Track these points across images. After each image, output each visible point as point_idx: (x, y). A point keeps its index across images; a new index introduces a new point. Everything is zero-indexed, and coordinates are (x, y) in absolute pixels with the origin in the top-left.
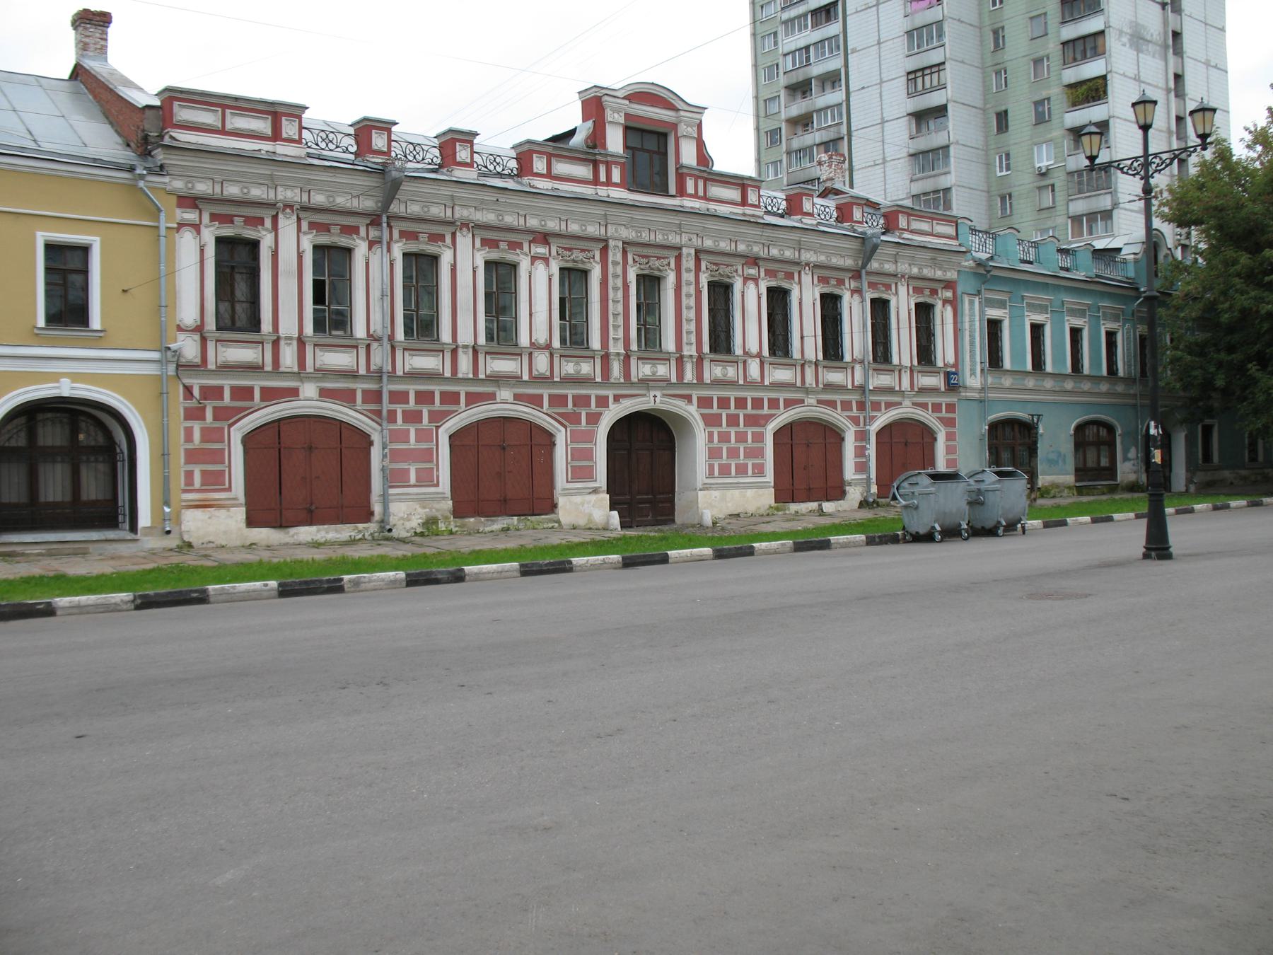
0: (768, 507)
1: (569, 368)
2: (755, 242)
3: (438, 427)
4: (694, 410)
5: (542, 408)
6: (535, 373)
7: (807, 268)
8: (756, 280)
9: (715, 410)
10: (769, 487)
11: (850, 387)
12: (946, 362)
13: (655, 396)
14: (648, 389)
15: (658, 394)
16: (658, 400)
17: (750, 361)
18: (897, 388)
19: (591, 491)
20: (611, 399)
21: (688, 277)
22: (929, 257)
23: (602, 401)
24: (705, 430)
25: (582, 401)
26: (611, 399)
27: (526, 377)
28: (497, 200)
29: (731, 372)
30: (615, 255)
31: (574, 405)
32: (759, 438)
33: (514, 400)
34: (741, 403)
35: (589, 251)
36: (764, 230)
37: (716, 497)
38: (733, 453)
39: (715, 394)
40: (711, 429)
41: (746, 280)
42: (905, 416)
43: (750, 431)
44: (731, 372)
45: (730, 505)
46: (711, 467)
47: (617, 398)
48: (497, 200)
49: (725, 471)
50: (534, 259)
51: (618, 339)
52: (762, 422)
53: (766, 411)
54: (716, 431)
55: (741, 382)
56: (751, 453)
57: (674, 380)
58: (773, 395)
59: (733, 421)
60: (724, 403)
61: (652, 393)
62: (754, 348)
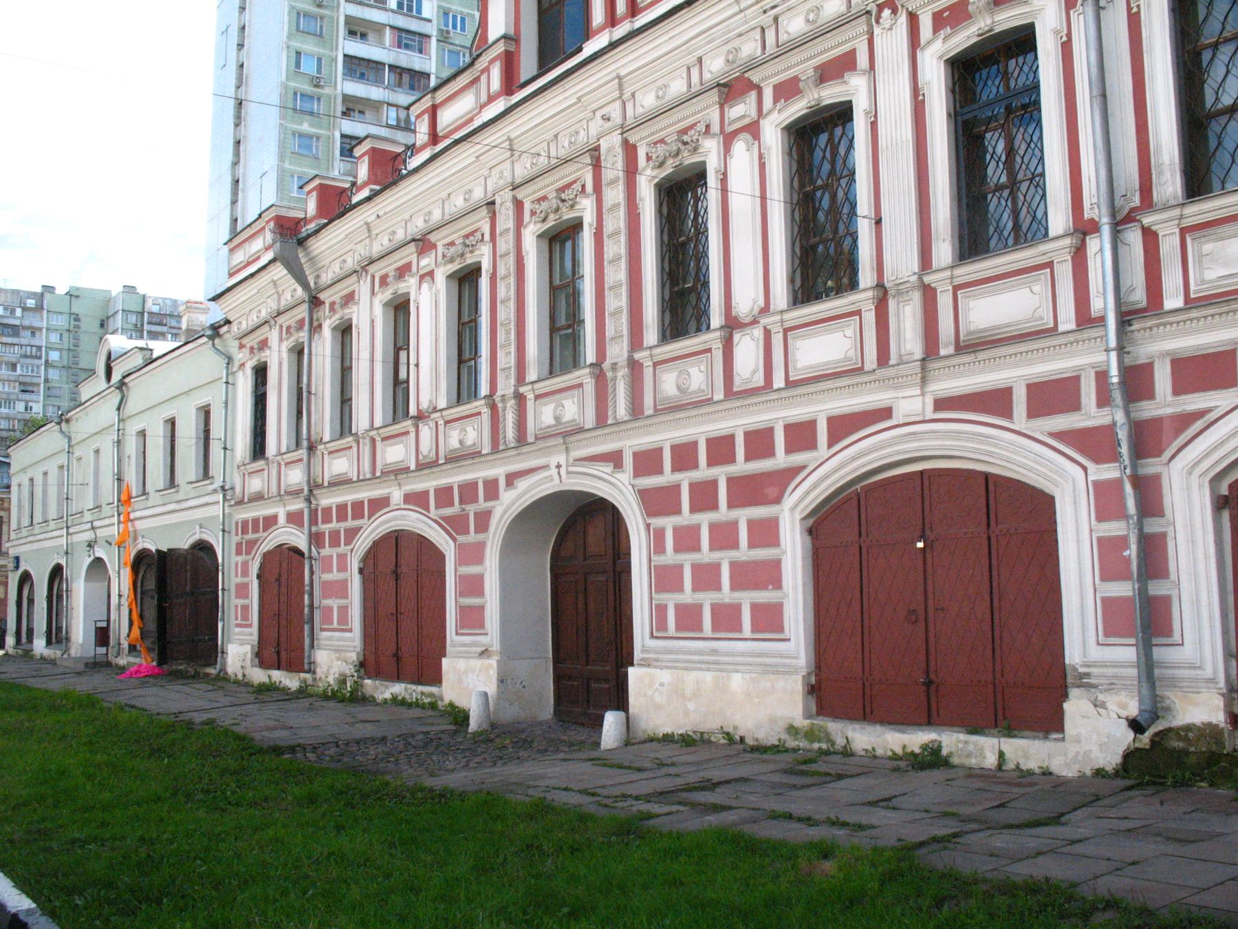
0: (782, 725)
1: (452, 439)
2: (740, 35)
3: (352, 550)
4: (627, 483)
5: (429, 512)
6: (421, 457)
7: (887, 13)
8: (753, 129)
9: (668, 477)
10: (796, 672)
11: (1067, 321)
13: (559, 466)
14: (547, 451)
15: (561, 459)
16: (563, 471)
17: (737, 337)
19: (480, 649)
20: (502, 482)
21: (615, 195)
23: (492, 488)
24: (648, 526)
25: (468, 492)
26: (502, 482)
27: (413, 467)
28: (378, 216)
29: (697, 377)
30: (506, 220)
31: (462, 502)
32: (766, 533)
33: (405, 502)
34: (721, 449)
35: (476, 231)
37: (662, 685)
38: (706, 577)
39: (665, 436)
40: (657, 522)
41: (728, 139)
43: (744, 516)
44: (697, 377)
45: (691, 706)
46: (661, 610)
47: (511, 479)
48: (378, 216)
49: (689, 619)
50: (422, 277)
51: (510, 368)
52: (771, 491)
53: (781, 459)
54: (668, 523)
55: (719, 395)
56: (746, 576)
57: (590, 420)
58: (798, 413)
59: (704, 497)
60: (684, 456)
61: (553, 461)
62: (746, 299)
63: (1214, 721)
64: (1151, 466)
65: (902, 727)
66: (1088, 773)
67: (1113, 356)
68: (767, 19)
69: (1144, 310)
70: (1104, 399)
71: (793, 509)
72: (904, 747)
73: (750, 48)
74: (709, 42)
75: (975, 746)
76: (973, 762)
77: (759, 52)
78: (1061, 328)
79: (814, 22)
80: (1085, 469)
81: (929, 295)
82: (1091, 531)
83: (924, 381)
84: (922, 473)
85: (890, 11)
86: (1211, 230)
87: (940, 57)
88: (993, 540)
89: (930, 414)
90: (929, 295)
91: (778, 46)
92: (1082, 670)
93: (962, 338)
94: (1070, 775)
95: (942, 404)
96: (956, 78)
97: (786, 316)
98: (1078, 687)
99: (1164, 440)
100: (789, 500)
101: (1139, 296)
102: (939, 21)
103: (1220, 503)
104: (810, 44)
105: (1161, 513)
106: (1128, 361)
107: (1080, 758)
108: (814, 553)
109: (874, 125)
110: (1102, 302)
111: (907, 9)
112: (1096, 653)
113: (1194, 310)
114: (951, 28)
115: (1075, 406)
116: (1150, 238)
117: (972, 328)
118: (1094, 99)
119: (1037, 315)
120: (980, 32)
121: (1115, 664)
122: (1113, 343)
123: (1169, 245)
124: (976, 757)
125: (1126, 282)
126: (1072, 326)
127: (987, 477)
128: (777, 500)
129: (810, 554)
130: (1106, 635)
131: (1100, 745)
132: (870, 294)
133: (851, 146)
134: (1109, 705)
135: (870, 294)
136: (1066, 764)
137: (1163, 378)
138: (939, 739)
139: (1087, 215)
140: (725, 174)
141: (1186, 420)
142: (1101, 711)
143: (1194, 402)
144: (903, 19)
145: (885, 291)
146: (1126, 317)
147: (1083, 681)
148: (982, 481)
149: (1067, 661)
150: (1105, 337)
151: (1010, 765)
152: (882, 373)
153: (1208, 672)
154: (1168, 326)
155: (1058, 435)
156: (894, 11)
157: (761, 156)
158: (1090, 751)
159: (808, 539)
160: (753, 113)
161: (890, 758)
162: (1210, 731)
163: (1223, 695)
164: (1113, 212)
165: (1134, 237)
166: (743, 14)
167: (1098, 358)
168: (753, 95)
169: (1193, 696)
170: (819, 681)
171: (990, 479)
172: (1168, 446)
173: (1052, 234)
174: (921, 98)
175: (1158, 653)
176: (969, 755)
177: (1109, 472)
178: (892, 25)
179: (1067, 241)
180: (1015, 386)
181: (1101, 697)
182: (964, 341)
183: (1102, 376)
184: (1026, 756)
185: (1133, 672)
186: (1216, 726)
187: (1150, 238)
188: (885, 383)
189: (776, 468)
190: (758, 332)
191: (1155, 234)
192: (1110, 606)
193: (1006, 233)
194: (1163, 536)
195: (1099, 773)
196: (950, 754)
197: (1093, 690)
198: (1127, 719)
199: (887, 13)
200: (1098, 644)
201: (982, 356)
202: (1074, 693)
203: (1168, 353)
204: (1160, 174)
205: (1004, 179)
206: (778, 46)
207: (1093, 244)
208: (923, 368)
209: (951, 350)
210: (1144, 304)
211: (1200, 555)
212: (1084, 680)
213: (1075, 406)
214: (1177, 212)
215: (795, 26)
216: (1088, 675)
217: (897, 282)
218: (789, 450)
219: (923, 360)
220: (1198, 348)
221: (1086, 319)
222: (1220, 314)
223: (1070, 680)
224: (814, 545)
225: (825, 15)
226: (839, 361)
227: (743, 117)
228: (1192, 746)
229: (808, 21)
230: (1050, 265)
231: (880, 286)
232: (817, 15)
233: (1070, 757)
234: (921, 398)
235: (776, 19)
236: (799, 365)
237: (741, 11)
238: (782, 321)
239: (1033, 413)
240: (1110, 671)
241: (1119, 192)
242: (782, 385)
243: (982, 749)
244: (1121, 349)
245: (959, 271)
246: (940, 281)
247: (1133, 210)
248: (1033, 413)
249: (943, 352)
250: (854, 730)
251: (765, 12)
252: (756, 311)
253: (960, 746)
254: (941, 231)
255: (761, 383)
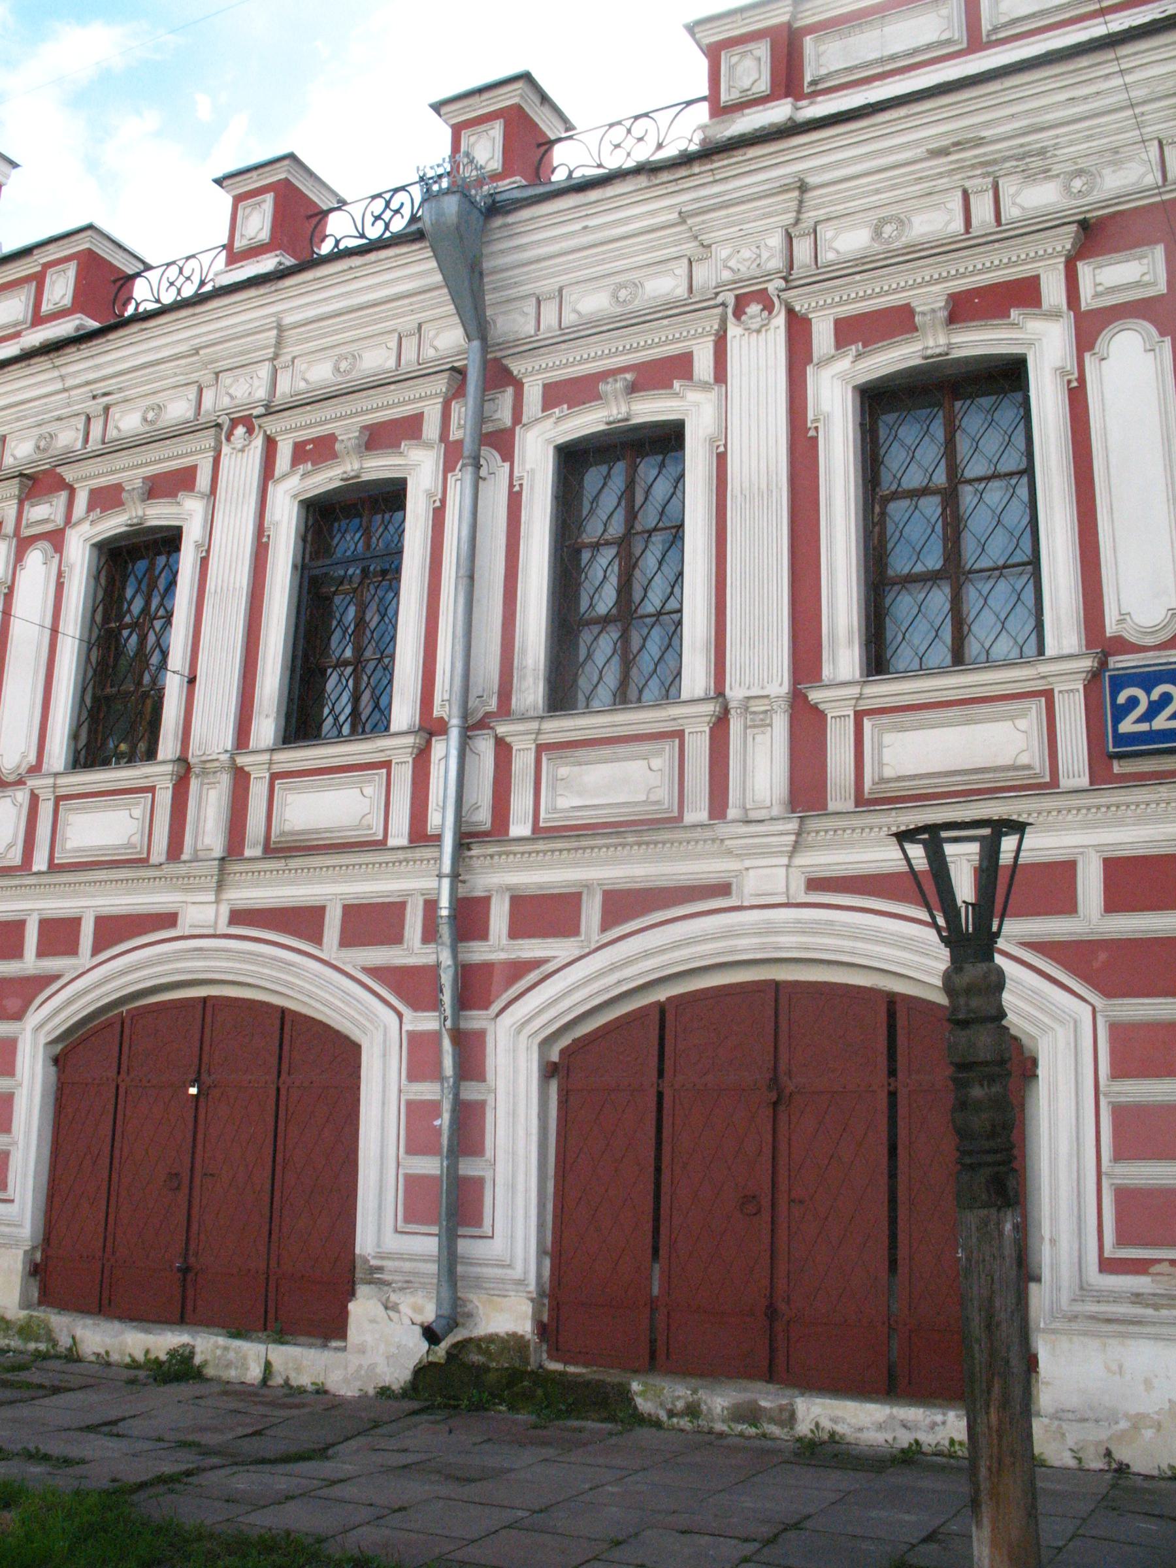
2: (59, 419)
7: (240, 430)
8: (56, 539)
10: (17, 1246)
11: (399, 835)
12: (1111, 627)
18: (697, 813)
22: (920, 152)
36: (64, 371)
42: (747, 947)
52: (12, 1004)
53: (30, 963)
58: (59, 905)
63: (520, 1332)
64: (476, 1020)
65: (147, 1325)
66: (371, 1392)
67: (446, 883)
68: (95, 407)
69: (486, 834)
70: (430, 935)
71: (38, 1029)
72: (147, 1352)
73: (68, 437)
74: (18, 420)
75: (236, 1353)
76: (232, 1374)
77: (79, 445)
78: (391, 842)
79: (152, 422)
80: (400, 1016)
81: (241, 778)
82: (400, 1091)
83: (220, 886)
84: (205, 1000)
85: (244, 430)
86: (568, 752)
87: (295, 496)
88: (283, 1092)
89: (223, 928)
90: (241, 778)
91: (104, 443)
92: (373, 1262)
93: (273, 838)
94: (349, 1394)
95: (239, 917)
96: (310, 523)
97: (62, 781)
98: (370, 1283)
99: (494, 988)
100: (34, 1017)
101: (483, 817)
102: (301, 454)
103: (549, 1071)
104: (143, 448)
105: (481, 1077)
106: (462, 891)
107: (363, 1372)
108: (58, 1089)
109: (204, 562)
110: (442, 818)
111: (265, 432)
112: (393, 1243)
113: (541, 842)
114: (313, 465)
115: (396, 938)
116: (503, 749)
117: (287, 827)
118: (460, 581)
119: (365, 822)
120: (345, 476)
121: (412, 1258)
122: (447, 867)
123: (522, 762)
124: (237, 1368)
125: (469, 800)
126: (404, 841)
127: (283, 1012)
128: (18, 1016)
129: (53, 1089)
130: (407, 1220)
131: (387, 1358)
132: (169, 768)
133: (172, 583)
134: (402, 1308)
135: (169, 768)
136: (346, 1380)
137: (499, 917)
138: (192, 1343)
139: (437, 712)
140: (11, 589)
141: (519, 969)
142: (391, 1313)
143: (531, 949)
144: (258, 442)
145: (188, 768)
146: (465, 839)
147: (375, 1278)
148: (279, 1015)
149: (358, 1251)
150: (439, 859)
151: (278, 1380)
152: (170, 869)
153: (517, 1273)
154: (511, 856)
155: (373, 972)
156: (250, 431)
157: (60, 574)
158: (375, 1365)
159: (53, 1070)
160: (59, 520)
161: (127, 1366)
162: (515, 1343)
163: (532, 1300)
164: (465, 715)
165: (485, 747)
166: (66, 395)
167: (430, 883)
168: (63, 495)
169: (499, 1299)
170: (46, 1257)
171: (288, 1019)
172: (498, 997)
173: (394, 728)
174: (265, 540)
175: (463, 1246)
176: (228, 1366)
177: (427, 1022)
178: (245, 446)
179: (410, 740)
180: (328, 904)
181: (394, 1297)
182: (275, 843)
183: (431, 906)
184: (298, 1370)
185: (433, 1268)
186: (522, 1337)
187: (503, 749)
188: (175, 884)
189: (21, 974)
190: (22, 796)
191: (508, 747)
192: (414, 1185)
193: (342, 718)
194: (482, 1105)
195: (384, 1392)
196: (205, 1363)
197: (386, 1288)
198: (422, 1326)
199: (240, 430)
200: (396, 1231)
201: (294, 863)
202: (362, 1290)
203: (508, 888)
204: (523, 678)
205: (348, 653)
206: (104, 443)
207: (438, 748)
208: (222, 870)
209: (257, 852)
210: (488, 826)
211: (521, 1133)
212: (376, 1276)
213: (396, 938)
214: (534, 725)
215: (129, 422)
216: (380, 1269)
217: (204, 758)
218: (41, 953)
219: (223, 859)
220: (540, 886)
221: (420, 836)
222: (569, 850)
223: (359, 1274)
224: (59, 1079)
225: (167, 417)
226: (117, 847)
227: (46, 521)
228: (493, 1360)
229: (145, 420)
230: (387, 765)
231: (182, 760)
232: (158, 415)
233: (351, 1370)
234: (214, 906)
235: (107, 409)
236: (69, 845)
237: (65, 390)
238: (55, 786)
239: (347, 941)
240: (408, 1266)
241: (474, 693)
242: (44, 868)
243: (245, 1358)
244: (455, 876)
245: (280, 756)
246: (255, 764)
247: (487, 713)
248: (347, 941)
249: (248, 853)
250: (85, 1327)
251: (94, 397)
252: (23, 770)
253: (219, 1352)
254: (265, 703)
255: (17, 861)
